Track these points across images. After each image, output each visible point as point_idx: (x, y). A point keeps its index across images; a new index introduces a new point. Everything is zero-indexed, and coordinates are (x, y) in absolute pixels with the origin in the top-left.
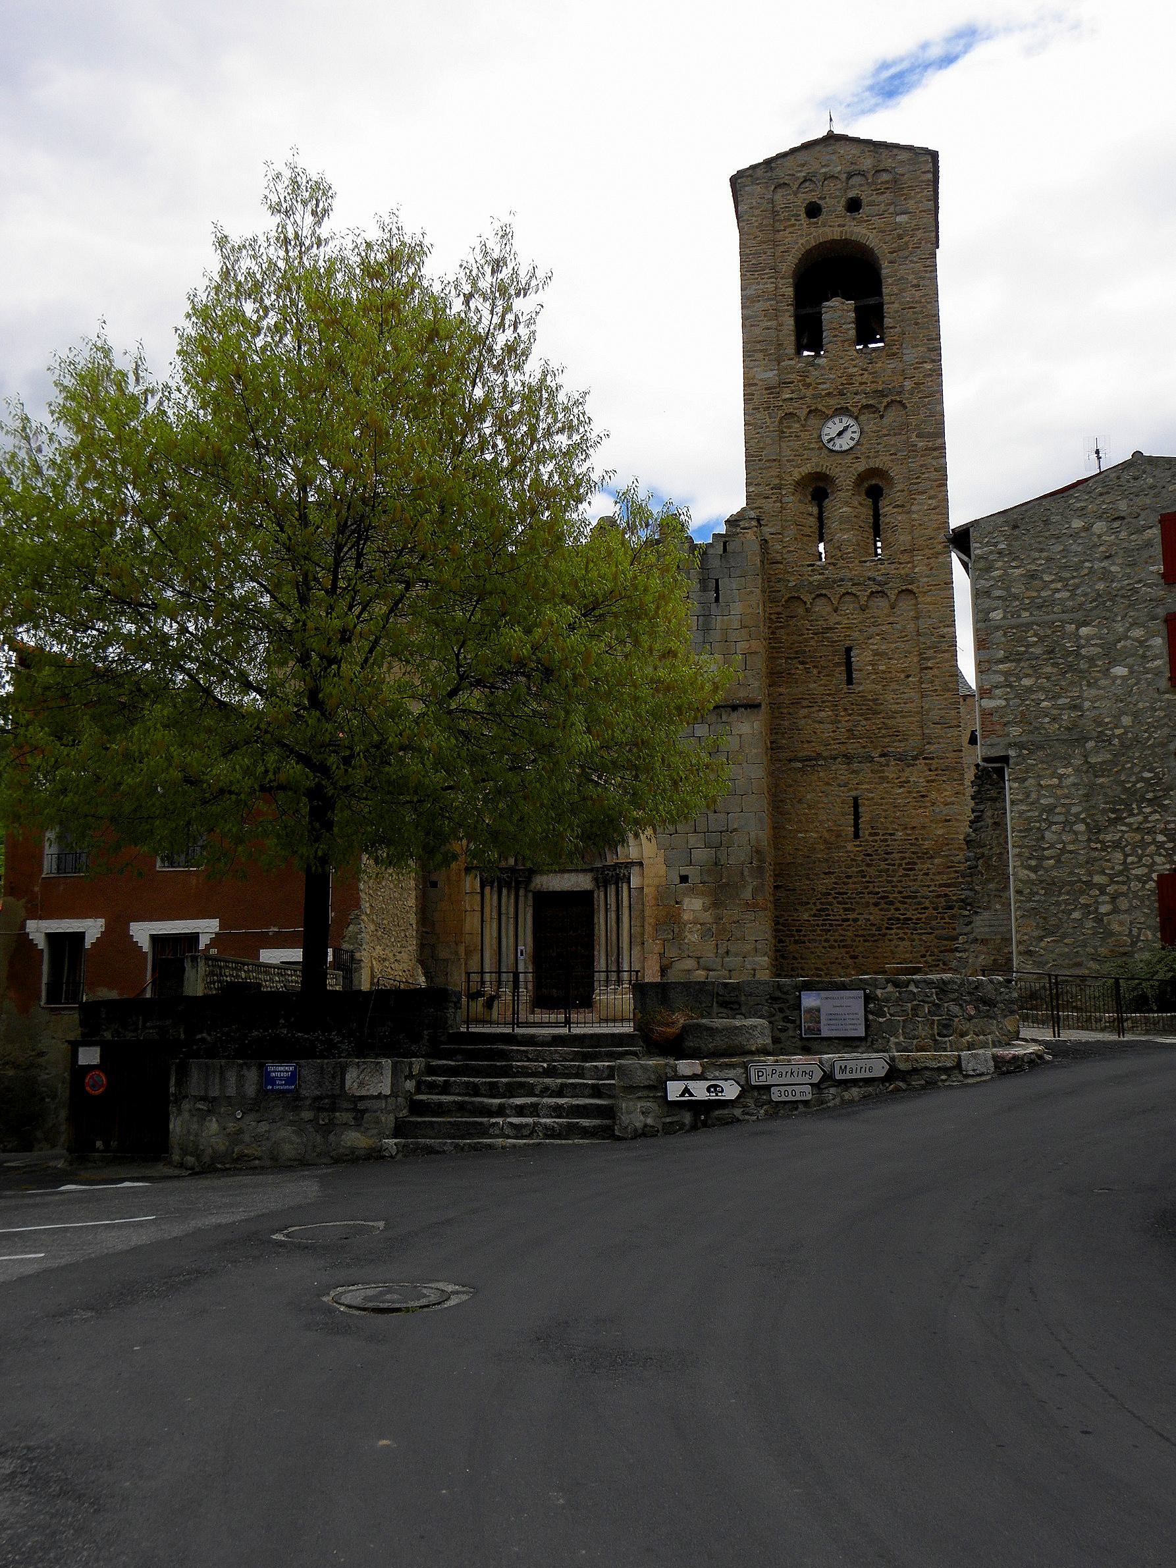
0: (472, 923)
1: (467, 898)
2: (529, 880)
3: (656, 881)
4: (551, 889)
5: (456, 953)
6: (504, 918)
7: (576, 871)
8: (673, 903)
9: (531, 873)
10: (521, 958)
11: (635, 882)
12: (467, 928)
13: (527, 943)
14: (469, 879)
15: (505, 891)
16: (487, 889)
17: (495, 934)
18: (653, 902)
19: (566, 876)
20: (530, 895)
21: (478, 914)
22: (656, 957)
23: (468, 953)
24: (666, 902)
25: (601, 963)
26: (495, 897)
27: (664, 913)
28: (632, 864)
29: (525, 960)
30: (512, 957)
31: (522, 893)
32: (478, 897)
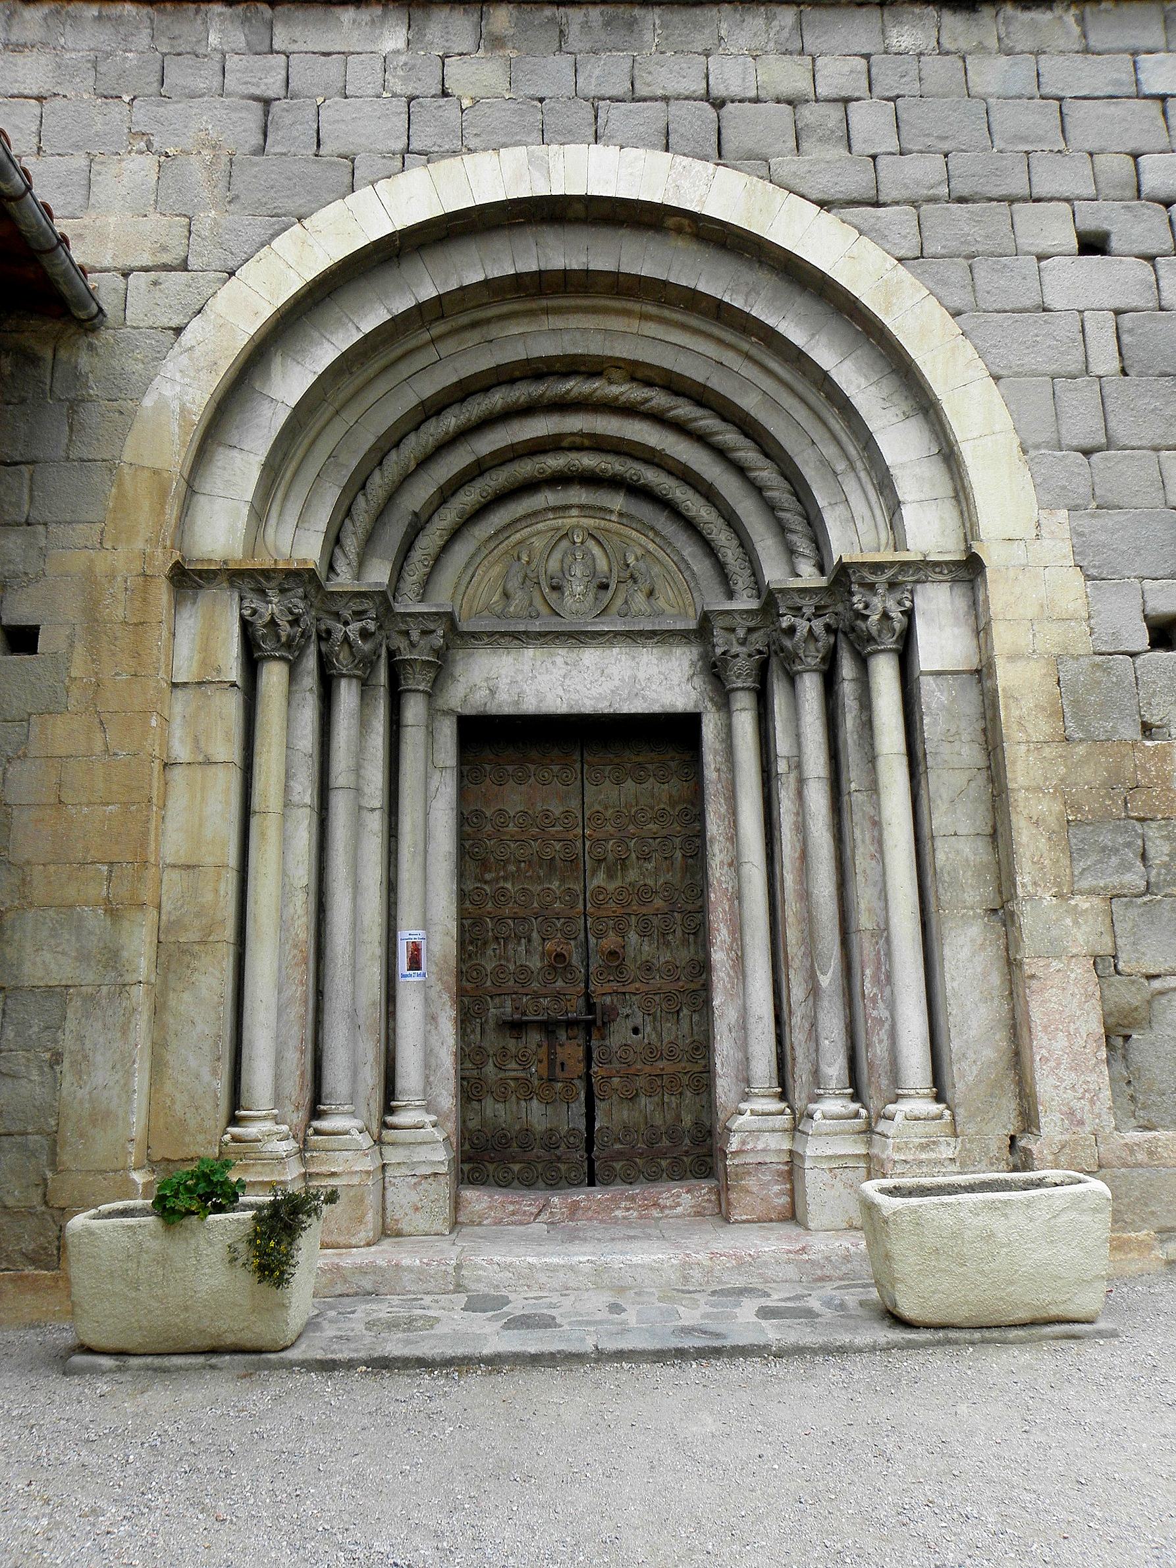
0: (197, 816)
1: (180, 705)
2: (440, 669)
3: (1050, 638)
4: (530, 706)
5: (112, 958)
6: (340, 805)
7: (634, 637)
8: (1132, 732)
9: (456, 636)
10: (409, 981)
11: (940, 642)
12: (173, 842)
13: (432, 915)
14: (190, 623)
15: (347, 696)
16: (273, 676)
17: (303, 874)
18: (1042, 728)
19: (590, 656)
20: (447, 732)
21: (227, 782)
22: (1081, 971)
23: (172, 956)
24: (1100, 727)
25: (742, 1006)
26: (308, 715)
27: (1092, 774)
28: (925, 568)
29: (426, 986)
30: (374, 974)
31: (414, 710)
32: (231, 705)
